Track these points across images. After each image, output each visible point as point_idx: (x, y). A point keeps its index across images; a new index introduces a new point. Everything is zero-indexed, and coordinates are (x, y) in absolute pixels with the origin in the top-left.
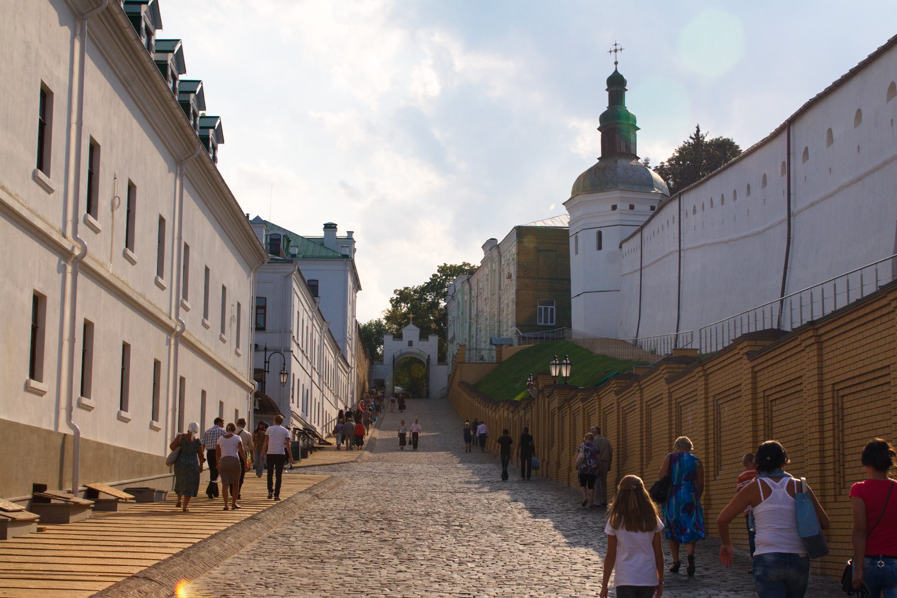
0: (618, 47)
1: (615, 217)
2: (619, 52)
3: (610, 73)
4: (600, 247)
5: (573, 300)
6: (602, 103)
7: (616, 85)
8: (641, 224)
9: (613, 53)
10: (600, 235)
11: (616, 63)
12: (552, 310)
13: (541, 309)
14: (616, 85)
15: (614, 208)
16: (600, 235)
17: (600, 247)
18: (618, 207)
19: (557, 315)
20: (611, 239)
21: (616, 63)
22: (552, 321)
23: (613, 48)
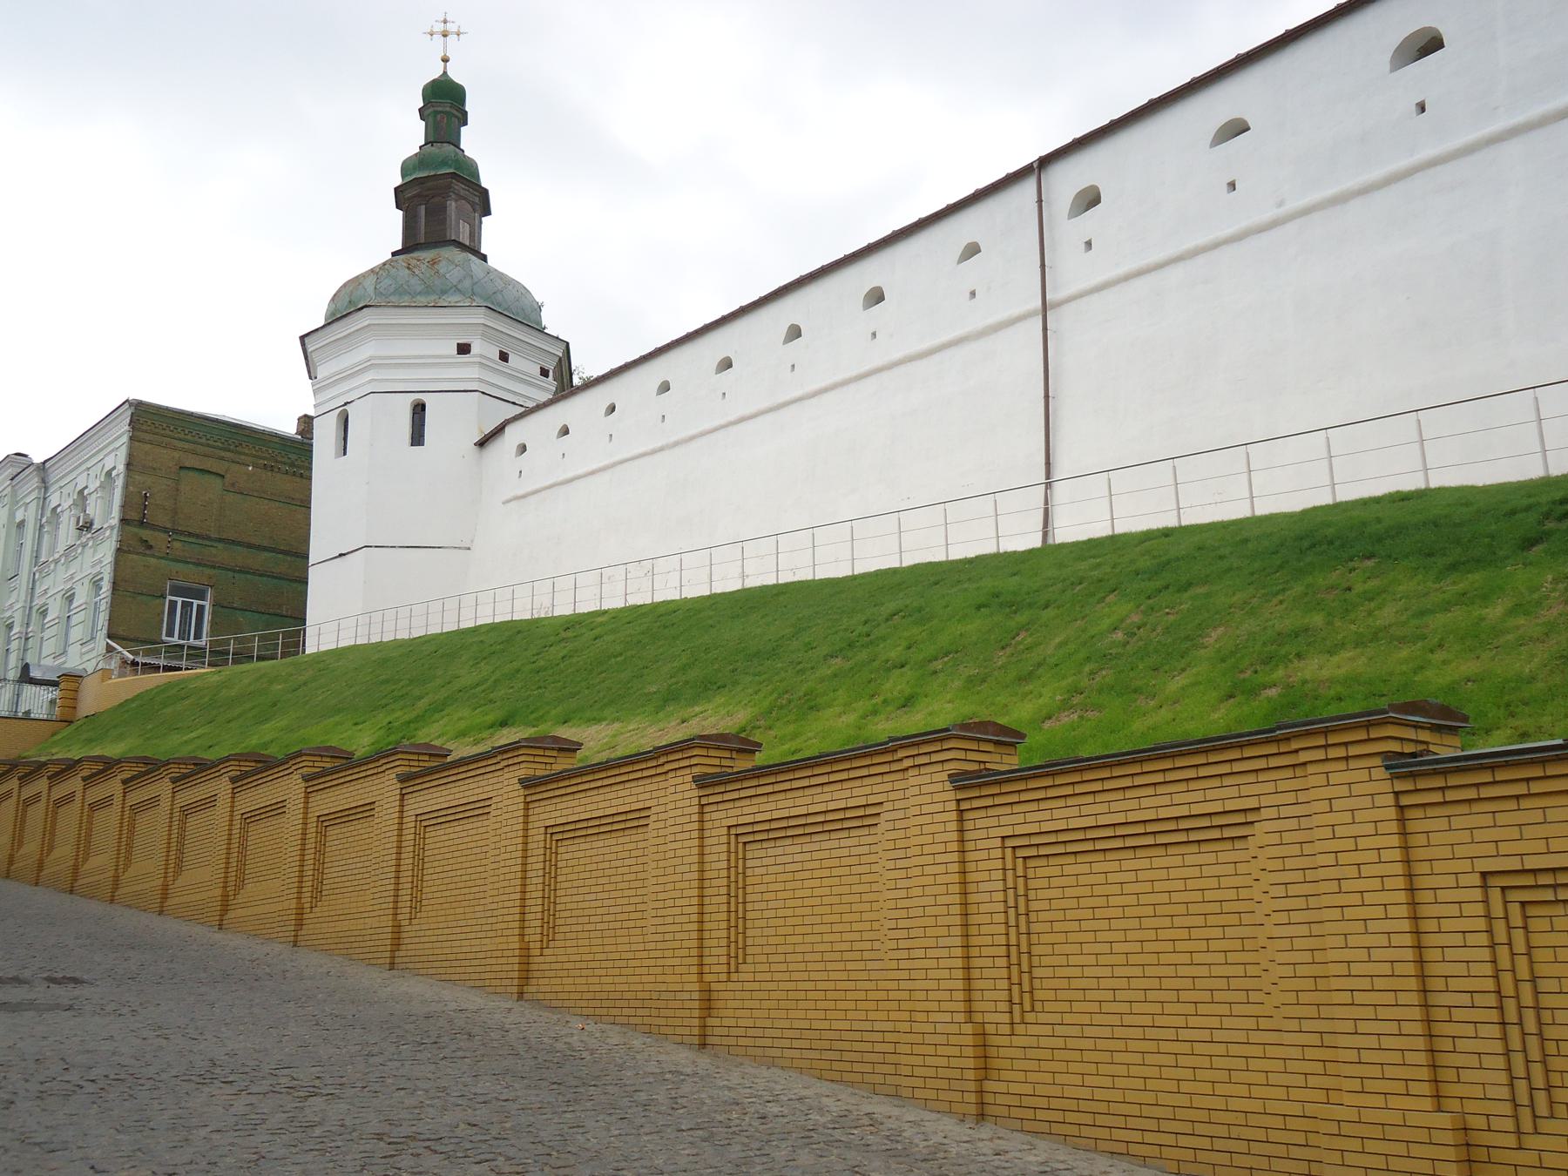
0: (451, 27)
1: (466, 372)
2: (452, 38)
3: (436, 73)
4: (417, 438)
5: (313, 574)
6: (411, 136)
7: (444, 105)
8: (531, 404)
9: (438, 39)
10: (419, 410)
11: (445, 60)
12: (201, 609)
13: (173, 604)
14: (444, 105)
15: (464, 349)
16: (419, 410)
17: (417, 438)
18: (474, 350)
19: (213, 623)
20: (453, 423)
21: (445, 60)
22: (198, 636)
23: (440, 27)
